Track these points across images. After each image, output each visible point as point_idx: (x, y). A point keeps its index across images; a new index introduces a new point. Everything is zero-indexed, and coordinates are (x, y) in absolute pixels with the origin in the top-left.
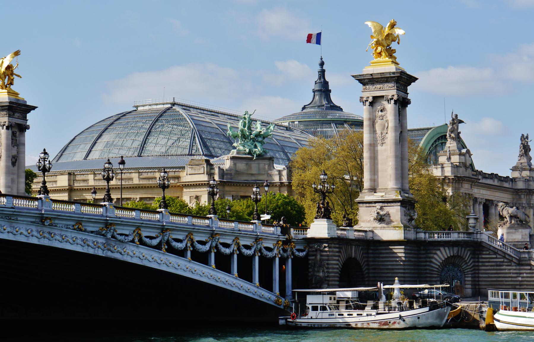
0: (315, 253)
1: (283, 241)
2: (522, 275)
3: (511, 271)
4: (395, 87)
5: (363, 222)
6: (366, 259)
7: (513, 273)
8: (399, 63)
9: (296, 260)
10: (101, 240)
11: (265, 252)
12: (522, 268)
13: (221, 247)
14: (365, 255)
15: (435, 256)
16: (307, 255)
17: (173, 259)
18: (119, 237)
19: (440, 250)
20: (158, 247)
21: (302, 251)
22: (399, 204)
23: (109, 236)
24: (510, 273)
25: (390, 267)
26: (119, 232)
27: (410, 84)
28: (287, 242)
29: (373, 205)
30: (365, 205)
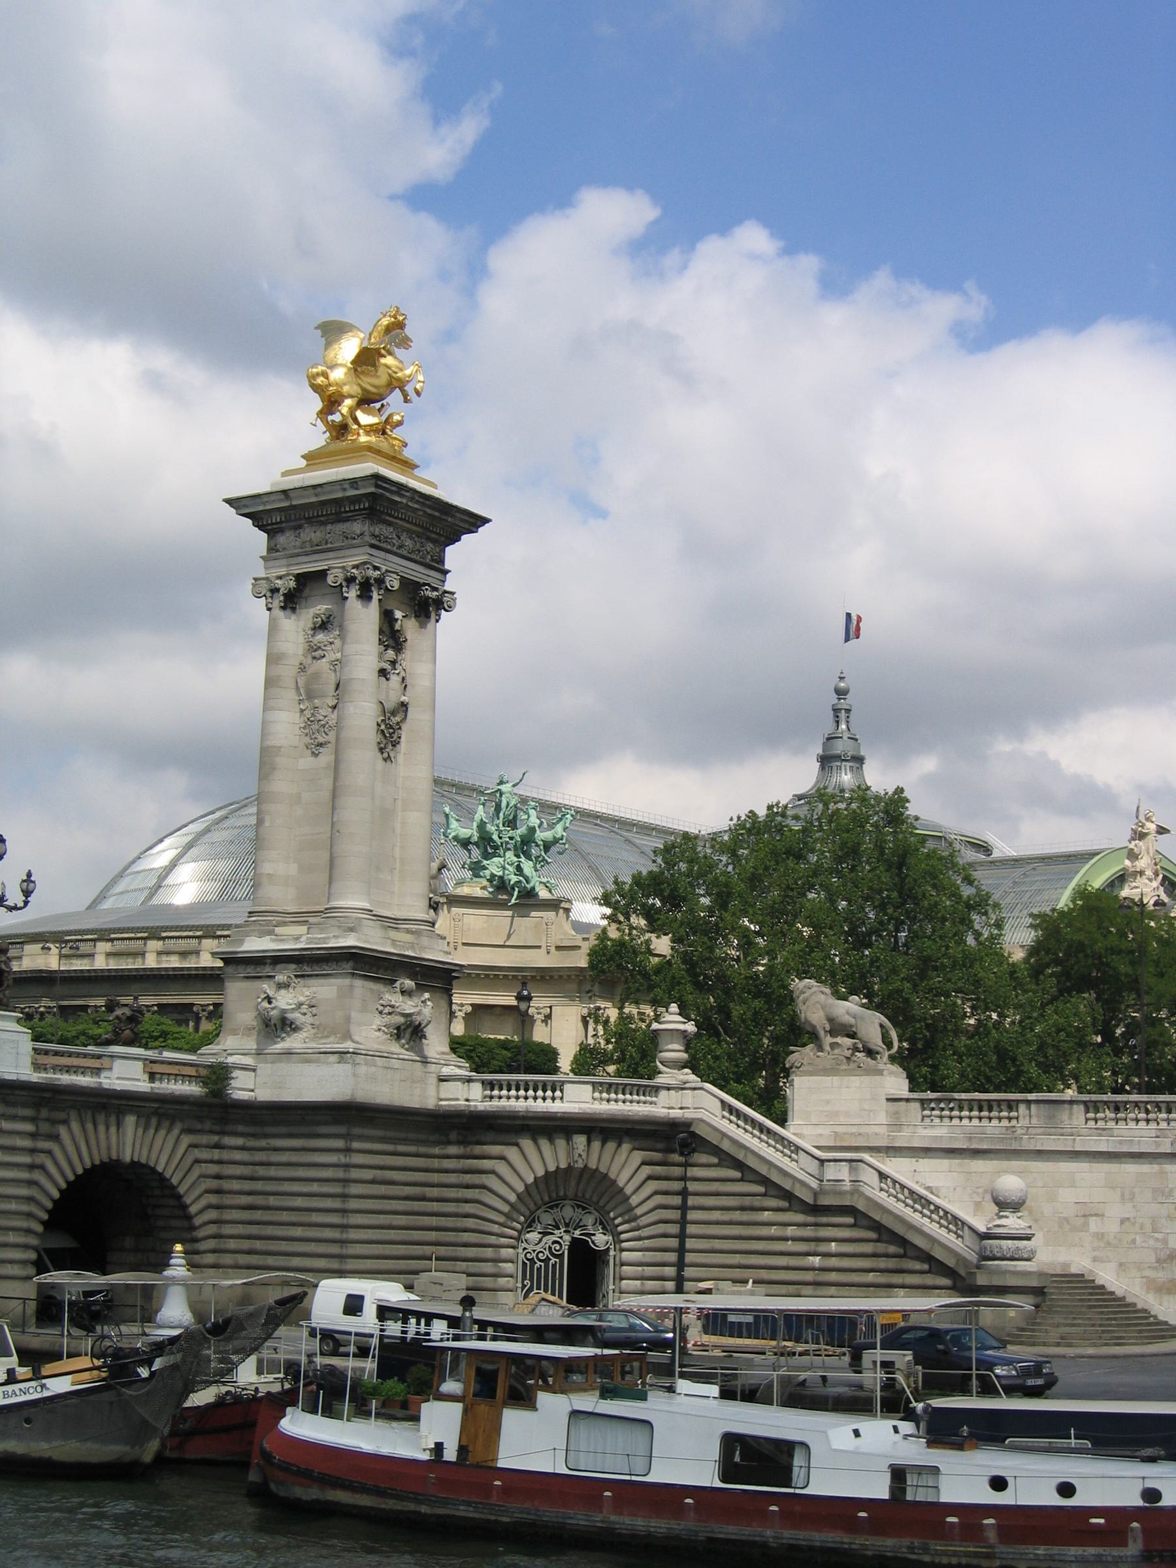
2: (823, 1248)
3: (790, 1231)
4: (367, 538)
5: (234, 1032)
6: (213, 1169)
7: (794, 1239)
8: (416, 461)
12: (824, 1220)
14: (204, 1154)
15: (501, 1168)
19: (517, 1145)
22: (348, 967)
24: (786, 1239)
25: (299, 1202)
27: (454, 539)
29: (267, 970)
30: (243, 971)
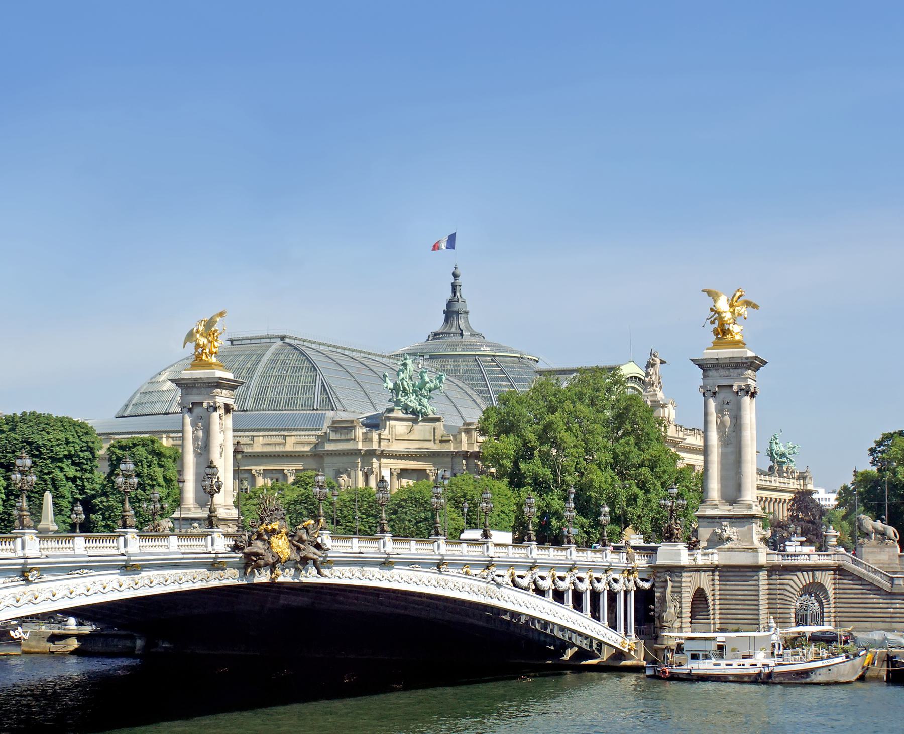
0: (662, 584)
1: (629, 571)
9: (639, 592)
10: (485, 585)
11: (614, 585)
13: (577, 581)
16: (653, 586)
17: (537, 600)
18: (499, 580)
20: (527, 589)
21: (647, 581)
23: (489, 579)
26: (498, 573)
28: (630, 572)
